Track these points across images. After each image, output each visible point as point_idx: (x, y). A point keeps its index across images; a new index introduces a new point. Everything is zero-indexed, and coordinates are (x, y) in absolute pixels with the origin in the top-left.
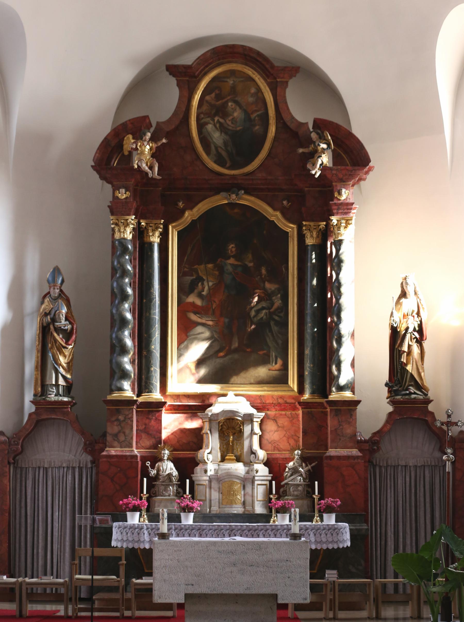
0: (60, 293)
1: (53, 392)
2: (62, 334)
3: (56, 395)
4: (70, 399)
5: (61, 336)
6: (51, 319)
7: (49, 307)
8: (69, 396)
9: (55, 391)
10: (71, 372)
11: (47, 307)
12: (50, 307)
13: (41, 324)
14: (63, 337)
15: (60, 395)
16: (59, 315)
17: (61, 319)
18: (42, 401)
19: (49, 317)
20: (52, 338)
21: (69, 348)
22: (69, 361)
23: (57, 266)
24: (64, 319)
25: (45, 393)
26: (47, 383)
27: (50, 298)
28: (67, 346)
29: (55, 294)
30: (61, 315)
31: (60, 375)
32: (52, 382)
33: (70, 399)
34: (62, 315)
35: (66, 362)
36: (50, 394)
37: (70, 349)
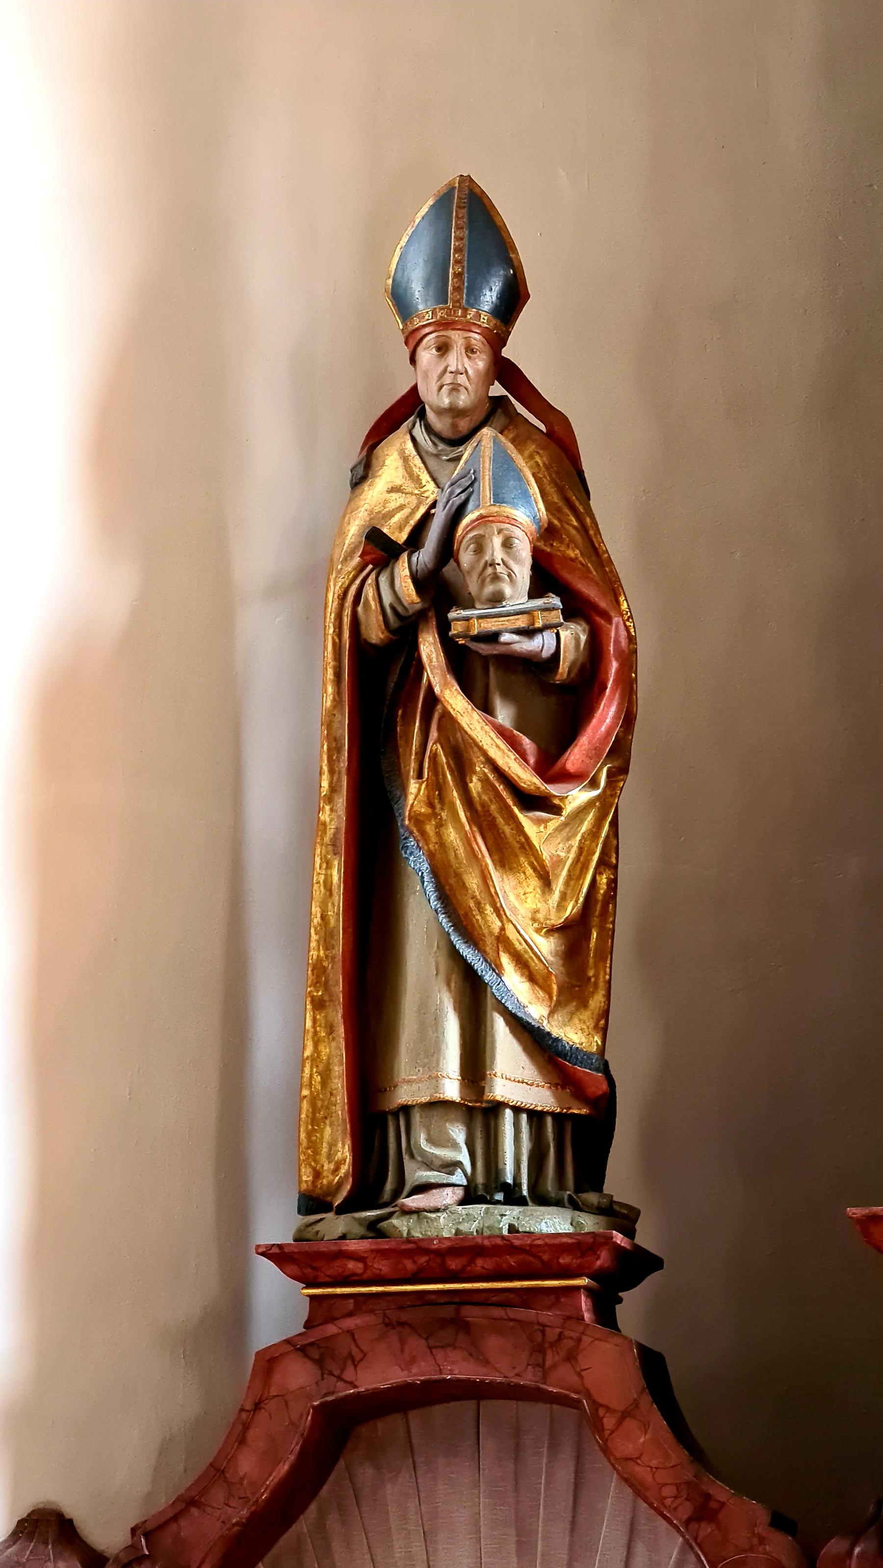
0: (497, 390)
1: (451, 1166)
2: (507, 695)
3: (470, 1196)
4: (589, 1223)
5: (504, 715)
6: (419, 581)
7: (413, 500)
8: (592, 1198)
9: (464, 1157)
10: (597, 1001)
11: (397, 500)
12: (420, 498)
13: (346, 634)
14: (522, 723)
15: (505, 1187)
16: (480, 547)
17: (496, 578)
18: (353, 1246)
19: (402, 569)
20: (434, 734)
21: (569, 808)
22: (571, 909)
23: (467, 181)
24: (523, 573)
25: (389, 1186)
26: (404, 1095)
27: (419, 432)
28: (553, 790)
29: (455, 388)
30: (497, 541)
31: (500, 1028)
32: (435, 1079)
33: (589, 1223)
34: (507, 544)
35: (558, 920)
36: (424, 1188)
37: (582, 811)
